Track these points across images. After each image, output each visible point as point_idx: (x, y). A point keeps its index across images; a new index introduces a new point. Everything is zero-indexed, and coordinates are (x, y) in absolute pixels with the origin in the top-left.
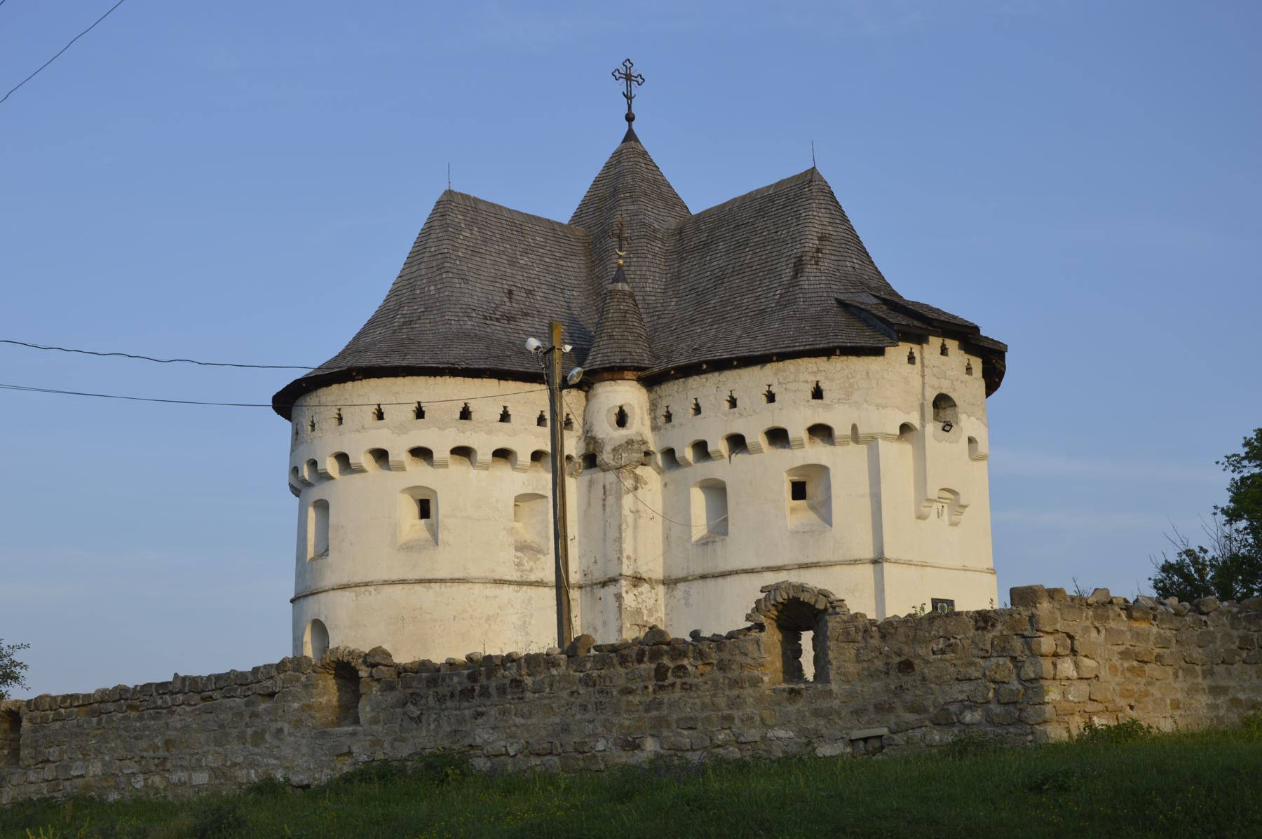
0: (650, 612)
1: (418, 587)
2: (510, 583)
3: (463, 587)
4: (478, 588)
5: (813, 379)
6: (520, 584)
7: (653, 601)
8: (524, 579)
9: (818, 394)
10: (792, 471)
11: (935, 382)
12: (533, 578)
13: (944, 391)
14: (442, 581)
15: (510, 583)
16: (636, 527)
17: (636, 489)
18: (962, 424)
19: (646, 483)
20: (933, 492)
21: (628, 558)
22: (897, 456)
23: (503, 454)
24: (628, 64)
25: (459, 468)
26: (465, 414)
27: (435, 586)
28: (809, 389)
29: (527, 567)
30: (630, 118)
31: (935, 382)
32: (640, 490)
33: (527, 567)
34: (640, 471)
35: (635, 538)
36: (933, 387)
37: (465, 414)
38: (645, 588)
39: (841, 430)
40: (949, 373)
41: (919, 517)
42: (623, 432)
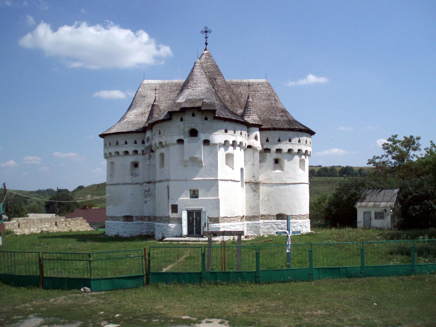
6: (131, 184)
9: (160, 133)
10: (160, 154)
12: (135, 182)
17: (149, 159)
20: (186, 158)
22: (175, 149)
24: (206, 28)
26: (117, 143)
27: (114, 186)
28: (158, 132)
30: (206, 44)
31: (189, 125)
32: (151, 160)
34: (152, 154)
36: (188, 127)
37: (117, 143)
38: (151, 185)
39: (164, 144)
40: (194, 122)
41: (185, 166)
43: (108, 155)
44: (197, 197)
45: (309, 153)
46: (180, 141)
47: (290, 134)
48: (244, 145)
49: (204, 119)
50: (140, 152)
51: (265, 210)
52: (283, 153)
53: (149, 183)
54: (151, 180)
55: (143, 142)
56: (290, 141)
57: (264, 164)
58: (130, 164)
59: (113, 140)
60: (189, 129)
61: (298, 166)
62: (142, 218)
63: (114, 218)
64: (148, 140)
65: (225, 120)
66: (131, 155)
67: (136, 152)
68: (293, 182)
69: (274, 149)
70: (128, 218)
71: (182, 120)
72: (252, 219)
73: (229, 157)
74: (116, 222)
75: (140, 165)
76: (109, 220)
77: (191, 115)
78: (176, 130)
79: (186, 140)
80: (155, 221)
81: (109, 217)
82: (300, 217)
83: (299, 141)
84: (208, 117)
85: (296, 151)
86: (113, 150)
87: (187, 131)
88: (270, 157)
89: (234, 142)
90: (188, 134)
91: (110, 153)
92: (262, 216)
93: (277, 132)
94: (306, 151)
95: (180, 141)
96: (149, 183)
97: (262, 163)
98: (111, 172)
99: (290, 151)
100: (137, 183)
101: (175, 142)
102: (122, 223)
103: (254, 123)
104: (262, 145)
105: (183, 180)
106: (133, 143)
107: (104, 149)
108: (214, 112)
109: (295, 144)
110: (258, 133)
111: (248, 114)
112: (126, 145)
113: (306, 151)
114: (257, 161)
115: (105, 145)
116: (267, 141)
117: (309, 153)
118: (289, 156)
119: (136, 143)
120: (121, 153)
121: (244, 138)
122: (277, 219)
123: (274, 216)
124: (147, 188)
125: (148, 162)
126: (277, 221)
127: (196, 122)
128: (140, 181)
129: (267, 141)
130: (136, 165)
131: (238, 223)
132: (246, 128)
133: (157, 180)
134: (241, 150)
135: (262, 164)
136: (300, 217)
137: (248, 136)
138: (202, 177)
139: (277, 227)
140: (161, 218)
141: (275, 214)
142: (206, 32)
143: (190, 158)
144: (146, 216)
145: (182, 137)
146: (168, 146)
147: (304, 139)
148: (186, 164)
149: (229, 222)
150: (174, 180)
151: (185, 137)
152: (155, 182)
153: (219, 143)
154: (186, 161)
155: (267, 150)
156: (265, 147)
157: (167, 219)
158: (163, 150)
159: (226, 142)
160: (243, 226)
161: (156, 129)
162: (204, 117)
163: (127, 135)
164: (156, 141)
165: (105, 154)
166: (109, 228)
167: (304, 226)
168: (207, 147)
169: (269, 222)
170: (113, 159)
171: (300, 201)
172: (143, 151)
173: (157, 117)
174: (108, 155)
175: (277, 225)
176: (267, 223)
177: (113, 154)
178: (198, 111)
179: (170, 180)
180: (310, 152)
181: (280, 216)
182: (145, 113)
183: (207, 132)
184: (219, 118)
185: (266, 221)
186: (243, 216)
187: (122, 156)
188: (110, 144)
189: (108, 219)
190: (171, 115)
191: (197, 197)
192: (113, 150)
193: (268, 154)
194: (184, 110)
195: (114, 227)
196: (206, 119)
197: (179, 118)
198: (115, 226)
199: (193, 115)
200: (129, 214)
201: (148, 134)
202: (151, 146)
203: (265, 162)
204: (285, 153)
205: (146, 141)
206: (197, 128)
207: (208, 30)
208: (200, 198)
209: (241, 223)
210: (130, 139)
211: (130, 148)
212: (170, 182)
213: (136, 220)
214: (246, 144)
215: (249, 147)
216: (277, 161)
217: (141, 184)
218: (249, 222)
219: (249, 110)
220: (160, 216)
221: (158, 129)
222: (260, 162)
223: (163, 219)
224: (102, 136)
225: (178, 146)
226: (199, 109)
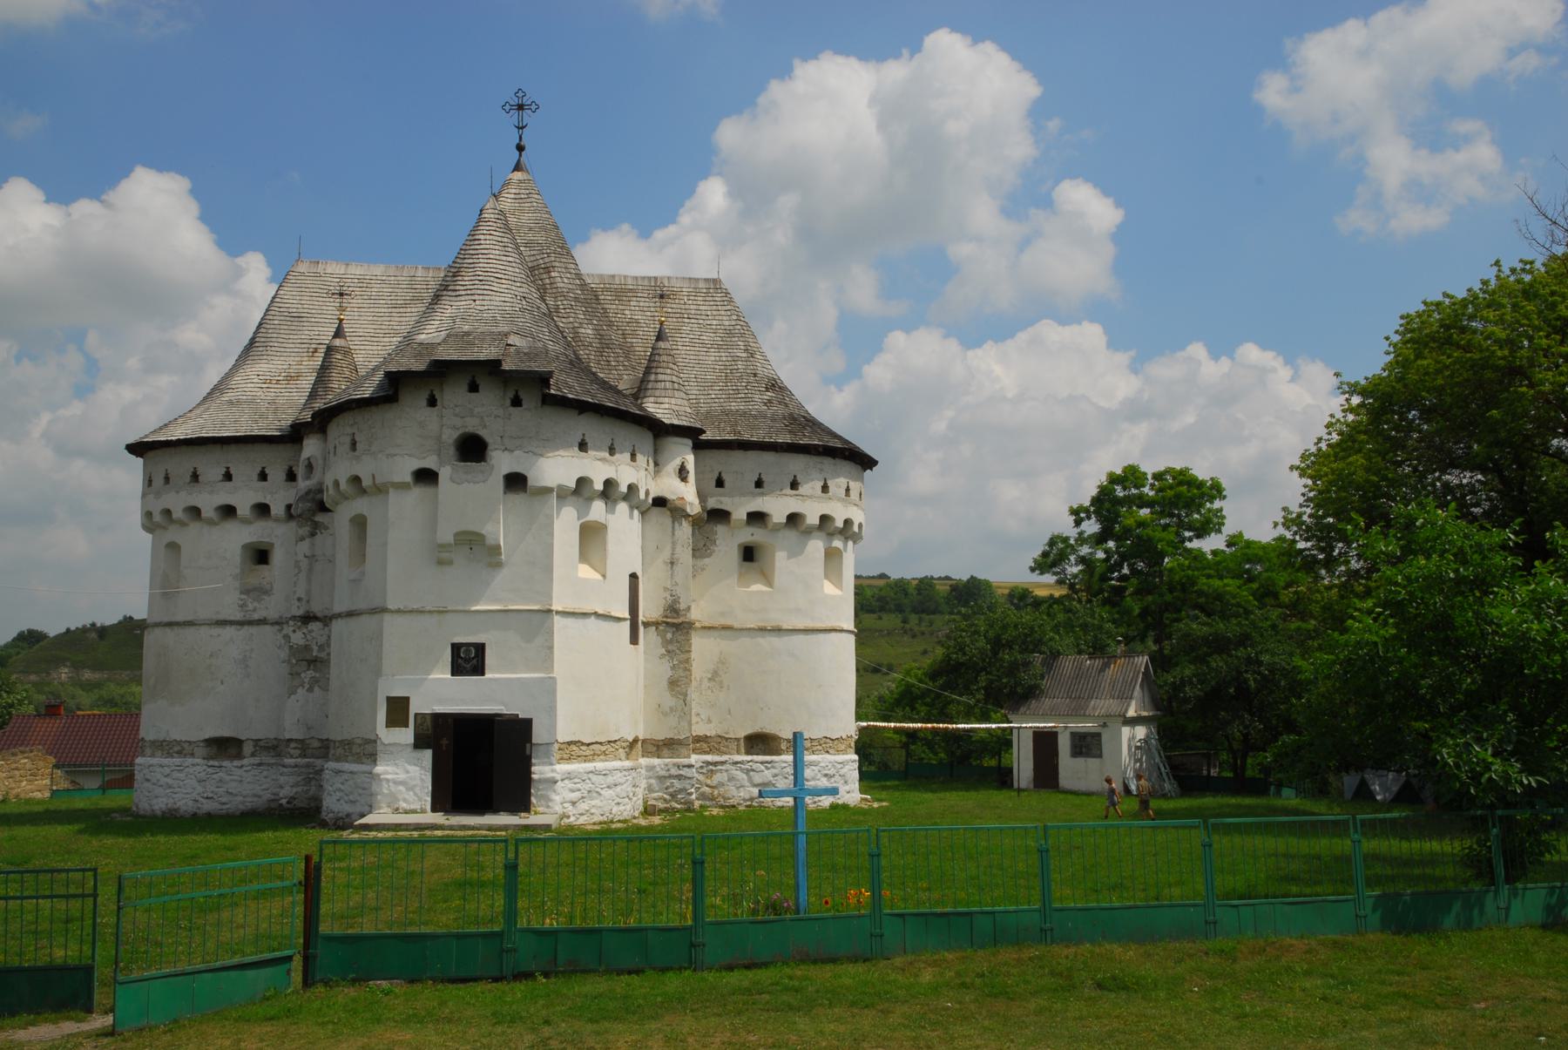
0: (321, 648)
1: (168, 630)
2: (231, 623)
3: (192, 629)
4: (204, 629)
5: (349, 430)
6: (241, 623)
7: (324, 639)
8: (248, 618)
9: (354, 445)
11: (458, 422)
12: (256, 616)
13: (470, 429)
14: (177, 624)
15: (231, 623)
16: (310, 570)
17: (313, 535)
18: (493, 462)
19: (326, 528)
20: (446, 536)
21: (299, 599)
23: (228, 511)
25: (194, 527)
26: (195, 477)
28: (348, 440)
29: (251, 607)
30: (520, 148)
31: (458, 422)
32: (319, 537)
33: (251, 607)
34: (320, 518)
35: (309, 580)
36: (454, 428)
39: (366, 482)
41: (440, 562)
42: (308, 483)
43: (157, 518)
44: (479, 670)
45: (856, 529)
46: (426, 477)
47: (796, 463)
48: (642, 496)
49: (508, 402)
50: (277, 509)
51: (709, 721)
52: (770, 526)
53: (307, 618)
54: (317, 608)
55: (291, 476)
56: (794, 485)
57: (706, 561)
58: (238, 551)
59: (179, 465)
60: (456, 435)
61: (820, 570)
62: (273, 748)
63: (165, 747)
64: (310, 467)
65: (581, 407)
66: (245, 521)
67: (262, 510)
68: (801, 626)
69: (740, 514)
70: (224, 747)
71: (432, 402)
72: (665, 751)
73: (591, 535)
74: (177, 761)
75: (277, 557)
76: (153, 755)
77: (465, 387)
78: (413, 437)
79: (445, 473)
80: (325, 757)
81: (153, 742)
82: (828, 744)
83: (825, 488)
84: (522, 395)
85: (813, 519)
86: (177, 501)
87: (451, 441)
88: (728, 542)
89: (609, 483)
90: (452, 451)
91: (167, 513)
92: (698, 739)
93: (753, 455)
94: (848, 522)
95: (426, 477)
96: (307, 618)
97: (702, 557)
98: (166, 581)
99: (794, 519)
100: (262, 622)
101: (409, 479)
102: (196, 765)
103: (676, 422)
104: (702, 496)
105: (430, 612)
106: (255, 477)
107: (144, 495)
108: (543, 379)
109: (810, 497)
110: (690, 460)
111: (657, 393)
112: (228, 484)
113: (848, 522)
114: (685, 555)
115: (149, 482)
116: (720, 483)
117: (856, 529)
118: (791, 535)
119: (263, 476)
120: (208, 512)
121: (643, 473)
122: (748, 753)
123: (738, 740)
124: (298, 638)
125: (304, 547)
126: (749, 758)
127: (481, 411)
128: (272, 614)
129: (720, 483)
130: (261, 556)
131: (617, 764)
132: (649, 436)
133: (337, 609)
134: (631, 517)
135: (701, 563)
136: (828, 744)
137: (656, 464)
138: (496, 601)
139: (750, 779)
140: (347, 744)
141: (742, 734)
142: (521, 107)
143: (456, 535)
144: (290, 740)
145: (430, 463)
146: (380, 490)
147: (838, 484)
148: (445, 555)
149: (586, 759)
150: (399, 611)
151: (442, 463)
152: (326, 620)
153: (560, 487)
154: (443, 547)
155: (719, 516)
156: (712, 503)
157: (369, 748)
158: (360, 506)
159: (582, 482)
160: (633, 773)
161: (339, 430)
162: (511, 394)
163: (233, 447)
164: (340, 471)
165: (148, 515)
166: (147, 784)
167: (838, 778)
168: (517, 499)
169: (723, 763)
170: (173, 534)
171: (823, 689)
172: (289, 507)
173: (339, 390)
174: (157, 518)
175: (747, 772)
176: (715, 764)
177: (178, 514)
178: (490, 374)
179: (384, 610)
180: (860, 526)
181: (760, 743)
182: (298, 376)
183: (519, 447)
184: (563, 403)
185: (709, 758)
186: (636, 741)
187: (210, 522)
188: (167, 479)
189: (148, 751)
190: (396, 385)
191: (479, 670)
192: (177, 501)
193: (720, 529)
194: (442, 371)
195: (169, 780)
196: (517, 402)
197: (425, 395)
198: (176, 775)
199: (474, 388)
200: (226, 733)
201: (311, 447)
202: (320, 490)
203: (710, 556)
204: (777, 528)
205: (300, 471)
206: (483, 433)
207: (526, 101)
208: (488, 676)
209: (628, 764)
210: (245, 465)
211: (244, 497)
212: (387, 617)
213: (253, 755)
214: (647, 493)
215: (660, 502)
216: (749, 554)
217: (277, 623)
218: (656, 761)
219: (661, 377)
220: (347, 736)
221: (349, 430)
222: (694, 556)
223: (356, 749)
224: (137, 449)
225: (419, 492)
226: (493, 367)
